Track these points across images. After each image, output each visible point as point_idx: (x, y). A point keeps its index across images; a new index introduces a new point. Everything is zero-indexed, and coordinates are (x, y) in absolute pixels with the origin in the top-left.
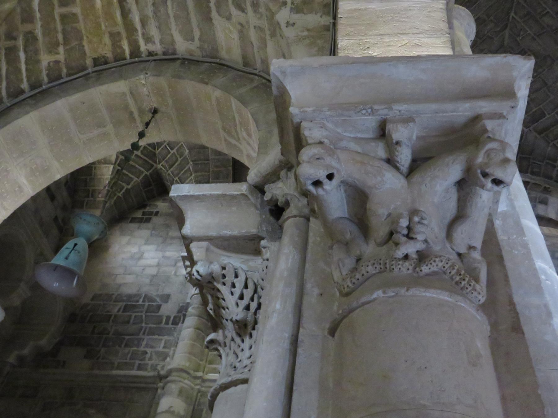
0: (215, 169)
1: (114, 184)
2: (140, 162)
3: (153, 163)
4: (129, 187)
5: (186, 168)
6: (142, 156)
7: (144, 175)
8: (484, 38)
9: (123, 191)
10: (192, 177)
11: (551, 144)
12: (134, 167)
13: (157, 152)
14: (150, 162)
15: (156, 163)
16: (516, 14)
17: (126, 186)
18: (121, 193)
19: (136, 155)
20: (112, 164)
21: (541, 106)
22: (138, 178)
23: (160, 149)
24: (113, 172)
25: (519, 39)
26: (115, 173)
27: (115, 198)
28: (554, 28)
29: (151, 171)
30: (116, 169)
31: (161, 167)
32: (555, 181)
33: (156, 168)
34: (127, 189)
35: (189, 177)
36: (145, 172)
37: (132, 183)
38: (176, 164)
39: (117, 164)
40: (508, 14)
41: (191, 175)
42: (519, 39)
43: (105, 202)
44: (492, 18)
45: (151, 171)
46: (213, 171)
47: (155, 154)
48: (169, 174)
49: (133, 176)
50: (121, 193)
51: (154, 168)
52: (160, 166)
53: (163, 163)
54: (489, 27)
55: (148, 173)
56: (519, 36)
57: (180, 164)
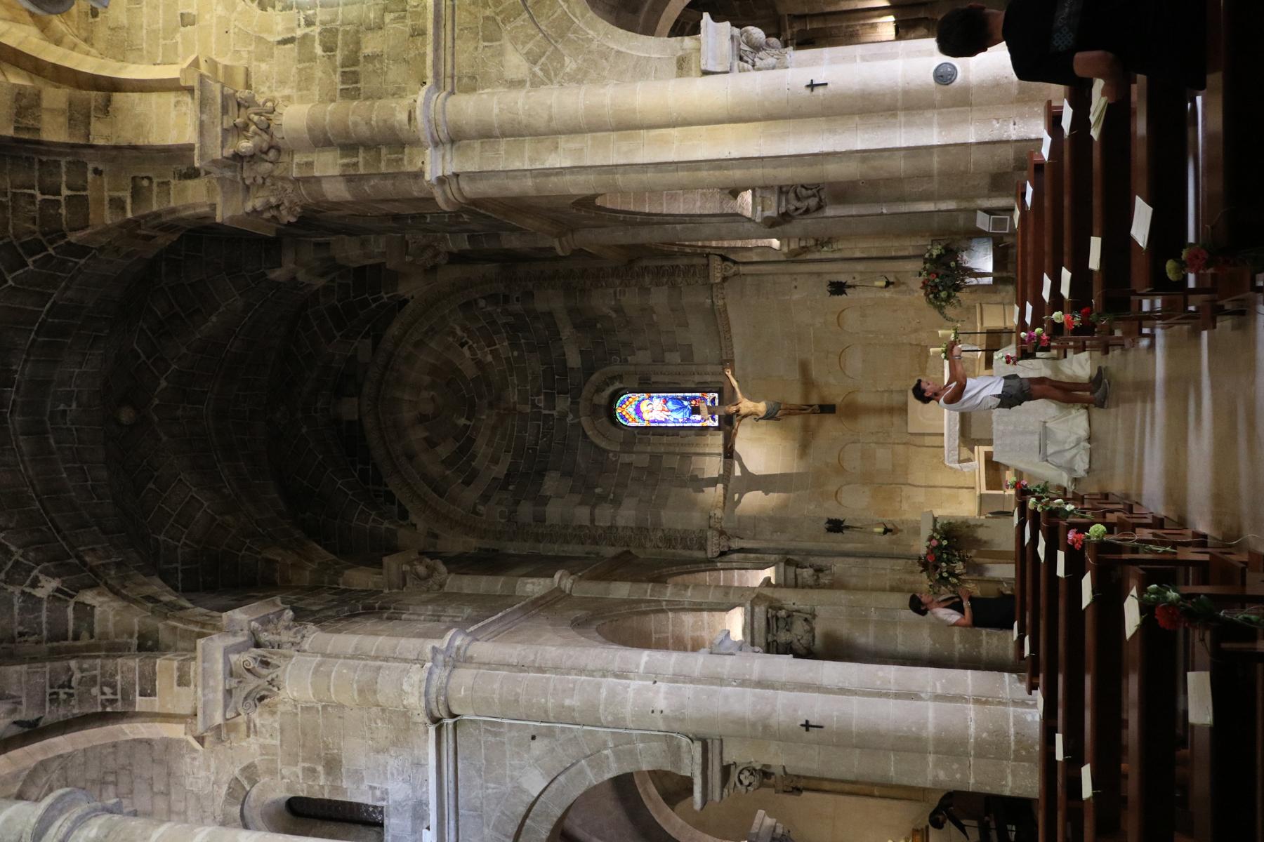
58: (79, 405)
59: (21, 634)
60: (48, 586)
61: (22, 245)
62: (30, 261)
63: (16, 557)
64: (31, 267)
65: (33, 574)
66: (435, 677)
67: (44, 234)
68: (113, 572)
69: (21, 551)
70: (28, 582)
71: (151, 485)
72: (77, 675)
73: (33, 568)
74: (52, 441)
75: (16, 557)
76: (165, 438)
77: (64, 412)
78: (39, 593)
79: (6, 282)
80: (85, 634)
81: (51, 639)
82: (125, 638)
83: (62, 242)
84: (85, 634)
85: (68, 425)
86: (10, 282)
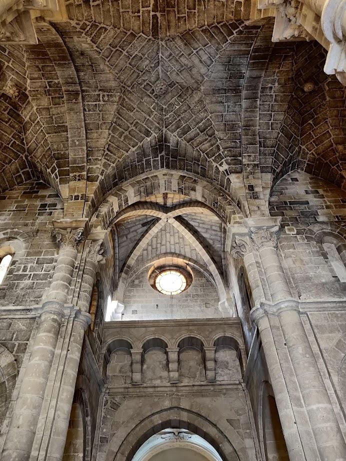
8: (144, 71)
11: (195, 149)
16: (162, 53)
21: (188, 123)
25: (169, 73)
28: (189, 67)
32: (201, 175)
40: (157, 54)
42: (169, 73)
44: (146, 56)
54: (146, 63)
56: (167, 71)
58: (279, 84)
59: (214, 179)
60: (225, 167)
61: (229, 25)
62: (234, 32)
63: (221, 152)
64: (235, 35)
65: (223, 160)
66: (258, 312)
67: (236, 21)
68: (249, 169)
69: (223, 150)
70: (220, 163)
71: (311, 122)
72: (219, 203)
73: (224, 158)
74: (258, 102)
75: (221, 152)
76: (328, 99)
77: (271, 88)
78: (221, 169)
79: (228, 41)
80: (228, 190)
81: (220, 185)
82: (235, 199)
83: (243, 25)
84: (228, 190)
85: (272, 93)
86: (229, 41)
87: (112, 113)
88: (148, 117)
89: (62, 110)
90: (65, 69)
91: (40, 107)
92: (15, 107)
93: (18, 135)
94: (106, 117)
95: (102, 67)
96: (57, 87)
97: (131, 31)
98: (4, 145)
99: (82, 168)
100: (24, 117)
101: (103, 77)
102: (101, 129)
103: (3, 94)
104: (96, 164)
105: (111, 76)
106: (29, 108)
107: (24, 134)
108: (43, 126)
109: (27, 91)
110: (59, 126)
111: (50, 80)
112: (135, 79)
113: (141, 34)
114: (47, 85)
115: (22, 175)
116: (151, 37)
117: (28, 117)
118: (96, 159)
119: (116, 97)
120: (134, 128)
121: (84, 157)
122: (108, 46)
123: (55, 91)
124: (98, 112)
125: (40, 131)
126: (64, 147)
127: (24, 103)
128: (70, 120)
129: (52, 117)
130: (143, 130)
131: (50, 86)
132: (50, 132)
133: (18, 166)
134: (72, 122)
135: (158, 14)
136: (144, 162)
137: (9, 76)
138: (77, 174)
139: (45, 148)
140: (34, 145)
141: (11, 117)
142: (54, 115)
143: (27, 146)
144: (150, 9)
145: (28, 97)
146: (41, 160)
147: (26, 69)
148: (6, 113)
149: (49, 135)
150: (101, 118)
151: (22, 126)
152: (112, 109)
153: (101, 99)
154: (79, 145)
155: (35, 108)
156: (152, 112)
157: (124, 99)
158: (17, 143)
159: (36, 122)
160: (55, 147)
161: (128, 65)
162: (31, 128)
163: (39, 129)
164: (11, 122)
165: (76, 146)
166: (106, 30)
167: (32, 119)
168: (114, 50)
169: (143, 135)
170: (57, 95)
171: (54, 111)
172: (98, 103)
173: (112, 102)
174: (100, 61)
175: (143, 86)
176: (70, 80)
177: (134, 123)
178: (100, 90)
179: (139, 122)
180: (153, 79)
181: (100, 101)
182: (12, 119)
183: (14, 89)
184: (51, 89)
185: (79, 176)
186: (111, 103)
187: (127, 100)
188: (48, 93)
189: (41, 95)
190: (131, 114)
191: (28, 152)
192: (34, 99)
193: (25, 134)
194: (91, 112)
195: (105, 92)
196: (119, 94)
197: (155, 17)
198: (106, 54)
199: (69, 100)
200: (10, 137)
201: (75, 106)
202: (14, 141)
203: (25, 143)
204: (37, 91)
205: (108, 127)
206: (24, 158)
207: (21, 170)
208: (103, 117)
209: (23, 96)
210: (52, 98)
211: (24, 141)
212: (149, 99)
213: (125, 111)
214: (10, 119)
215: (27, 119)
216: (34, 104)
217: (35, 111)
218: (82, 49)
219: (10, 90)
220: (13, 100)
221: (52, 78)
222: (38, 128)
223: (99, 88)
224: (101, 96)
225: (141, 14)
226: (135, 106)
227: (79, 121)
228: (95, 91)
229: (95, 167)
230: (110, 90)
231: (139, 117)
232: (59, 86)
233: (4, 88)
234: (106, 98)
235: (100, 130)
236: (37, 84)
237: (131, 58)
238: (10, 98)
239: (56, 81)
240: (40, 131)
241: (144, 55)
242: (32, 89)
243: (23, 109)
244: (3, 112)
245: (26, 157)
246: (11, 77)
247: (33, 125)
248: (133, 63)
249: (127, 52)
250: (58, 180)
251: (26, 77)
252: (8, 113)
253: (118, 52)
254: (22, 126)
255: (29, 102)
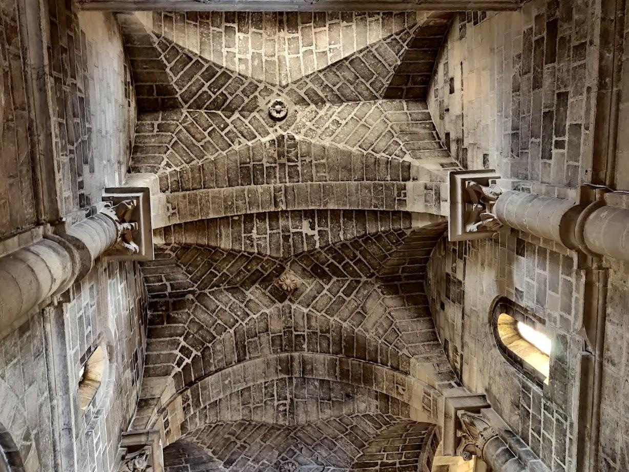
0: (199, 197)
1: (175, 50)
2: (194, 88)
3: (189, 104)
4: (168, 70)
5: (191, 155)
6: (200, 92)
7: (178, 90)
9: (165, 62)
10: (185, 165)
12: (190, 80)
13: (203, 111)
14: (192, 101)
15: (189, 108)
17: (169, 66)
18: (164, 59)
19: (204, 84)
20: (201, 52)
22: (176, 83)
23: (206, 116)
24: (192, 52)
26: (190, 55)
27: (160, 50)
29: (180, 99)
30: (192, 57)
31: (184, 115)
33: (183, 107)
34: (166, 67)
35: (181, 157)
36: (180, 92)
37: (171, 74)
38: (192, 138)
39: (200, 59)
40: (334, 465)
41: (188, 163)
43: (158, 36)
45: (180, 99)
46: (196, 195)
47: (200, 108)
48: (178, 126)
49: (179, 76)
50: (164, 59)
51: (183, 104)
52: (185, 112)
53: (190, 119)
55: (178, 96)
57: (194, 144)
87: (264, 419)
88: (251, 459)
89: (265, 350)
90: (326, 367)
91: (269, 319)
92: (265, 281)
93: (225, 281)
94: (258, 412)
95: (328, 411)
96: (296, 345)
97: (367, 446)
98: (215, 264)
99: (197, 405)
100: (251, 290)
101: (312, 408)
102: (243, 409)
103: (285, 268)
104: (200, 419)
105: (313, 418)
106: (266, 301)
107: (227, 287)
108: (244, 325)
109: (290, 303)
110: (245, 346)
111: (306, 340)
112: (304, 441)
113: (362, 453)
114: (299, 333)
115: (160, 284)
116: (356, 461)
117: (252, 298)
118: (206, 416)
119: (284, 420)
120: (238, 445)
121: (210, 400)
122: (354, 424)
123: (290, 341)
124: (264, 400)
125: (236, 317)
126: (219, 361)
127: (271, 293)
128: (254, 365)
129: (256, 336)
130: (234, 457)
131: (297, 336)
132: (238, 336)
133: (180, 281)
134: (252, 368)
135: (378, 467)
136: (184, 464)
137: (309, 284)
138: (190, 402)
139: (213, 327)
140: (214, 307)
141: (252, 274)
142: (259, 338)
143: (210, 293)
144: (385, 460)
145: (281, 302)
146: (192, 321)
147: (323, 313)
148: (259, 268)
149: (233, 335)
150: (258, 405)
151: (238, 285)
152: (268, 418)
153: (281, 402)
154: (224, 385)
155: (267, 311)
156: (258, 463)
157: (280, 430)
158: (215, 279)
159: (247, 310)
160: (218, 347)
161: (324, 436)
162: (237, 301)
163: (238, 316)
164: (244, 272)
165: (223, 380)
166: (377, 429)
167: (251, 304)
168: (348, 428)
169: (226, 458)
170: (284, 343)
171: (264, 338)
172: (276, 398)
173: (277, 417)
174: (337, 413)
175: (293, 448)
176: (309, 367)
177: (245, 445)
178: (292, 400)
179: (247, 450)
180: (301, 459)
181: (279, 400)
182: (249, 274)
183: (292, 286)
184: (293, 336)
185: (189, 405)
186: (275, 415)
187: (278, 433)
188: (288, 330)
189: (284, 322)
190: (258, 440)
191: (199, 295)
192: (279, 311)
193: (227, 290)
194: (263, 390)
195: (290, 406)
196: (287, 424)
197: (376, 464)
198: (345, 420)
199: (280, 361)
200: (225, 271)
201: (272, 370)
202: (217, 276)
203: (213, 289)
204: (291, 317)
205: (245, 418)
206: (191, 289)
207: (171, 284)
208: (257, 407)
209: (280, 295)
210: (281, 336)
211: (215, 288)
212: (276, 456)
213: (262, 432)
214: (249, 271)
215: (249, 295)
216: (271, 309)
217: (263, 311)
218: (357, 399)
219: (290, 279)
220: (275, 279)
221: (309, 343)
222: (239, 313)
223: (296, 400)
224: (284, 402)
225: (382, 453)
226: (268, 443)
227: (254, 378)
228: (291, 393)
229: (197, 420)
230: (293, 413)
231: (254, 448)
232: (298, 348)
233: (292, 272)
234: (281, 408)
235: (241, 408)
236: (301, 320)
237: (334, 440)
238: (278, 276)
239: (305, 346)
240: (236, 317)
241: (335, 452)
242: (292, 311)
243: (263, 291)
244: (260, 264)
245: (193, 292)
246: (309, 286)
247: (243, 305)
248: (326, 440)
249: (342, 438)
250: (178, 369)
251: (310, 308)
252: (257, 270)
253: (344, 430)
254: (238, 285)
255: (275, 303)
